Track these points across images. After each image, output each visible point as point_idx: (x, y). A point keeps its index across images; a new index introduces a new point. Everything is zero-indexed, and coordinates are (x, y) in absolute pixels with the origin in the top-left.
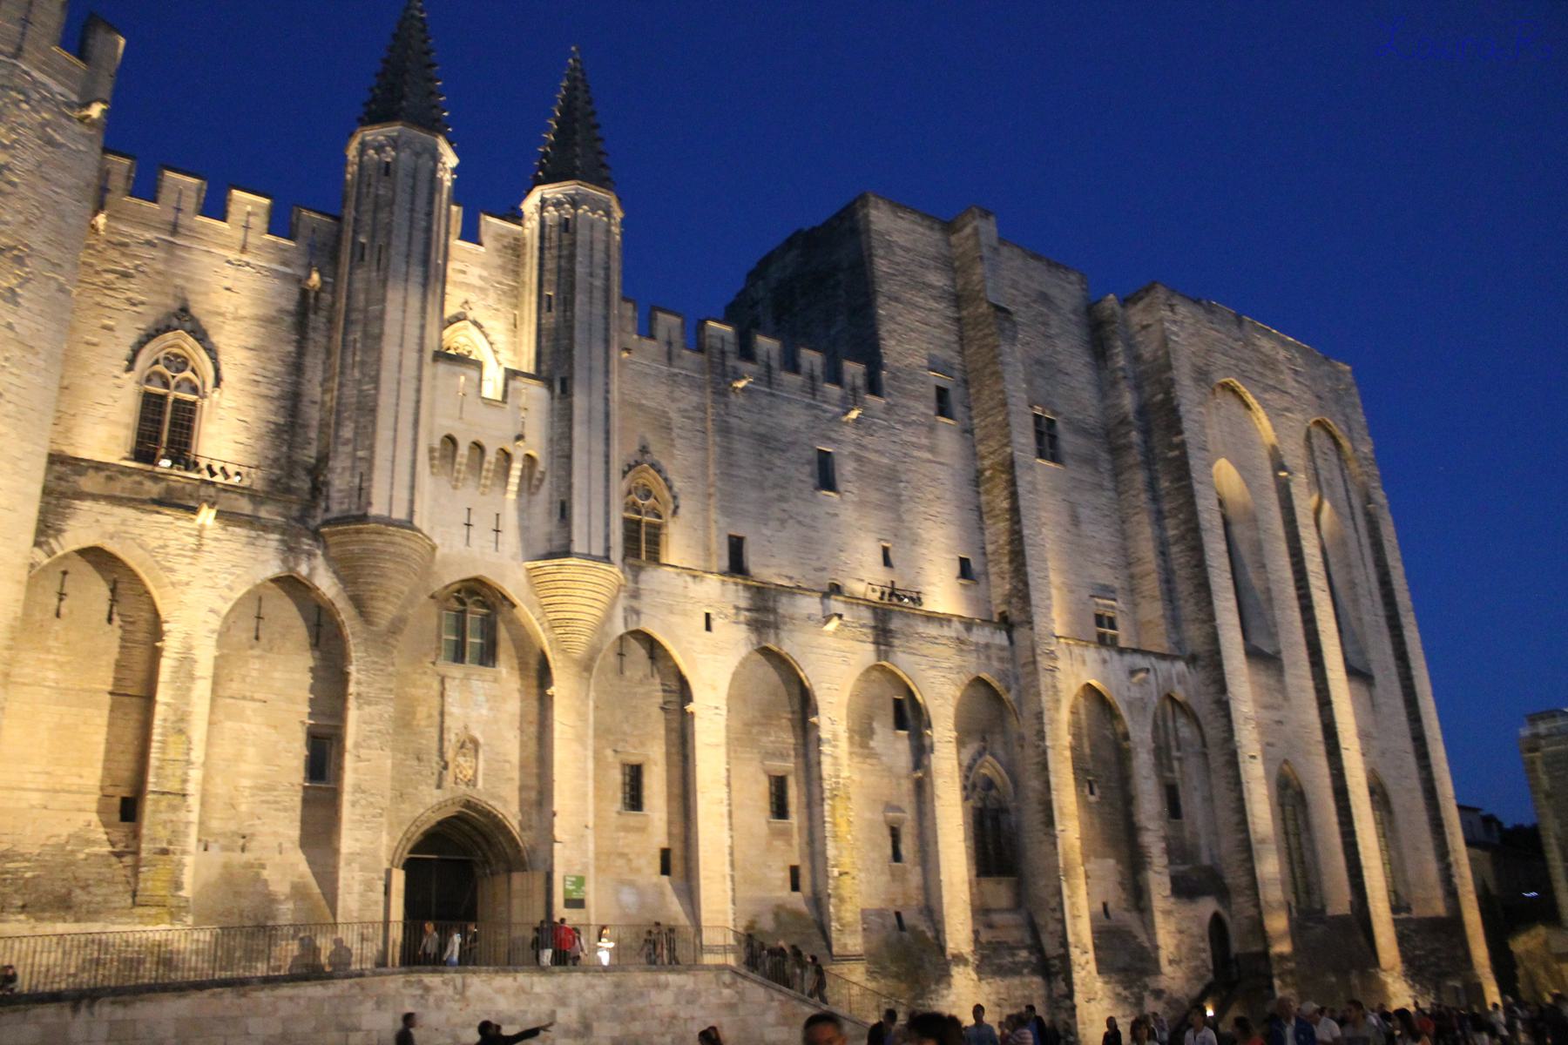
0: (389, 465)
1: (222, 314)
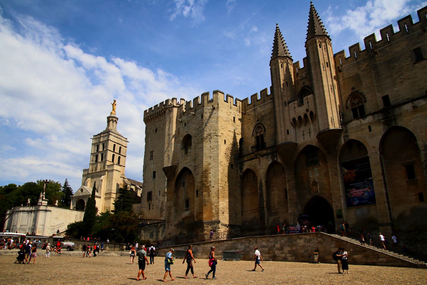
1: (263, 116)
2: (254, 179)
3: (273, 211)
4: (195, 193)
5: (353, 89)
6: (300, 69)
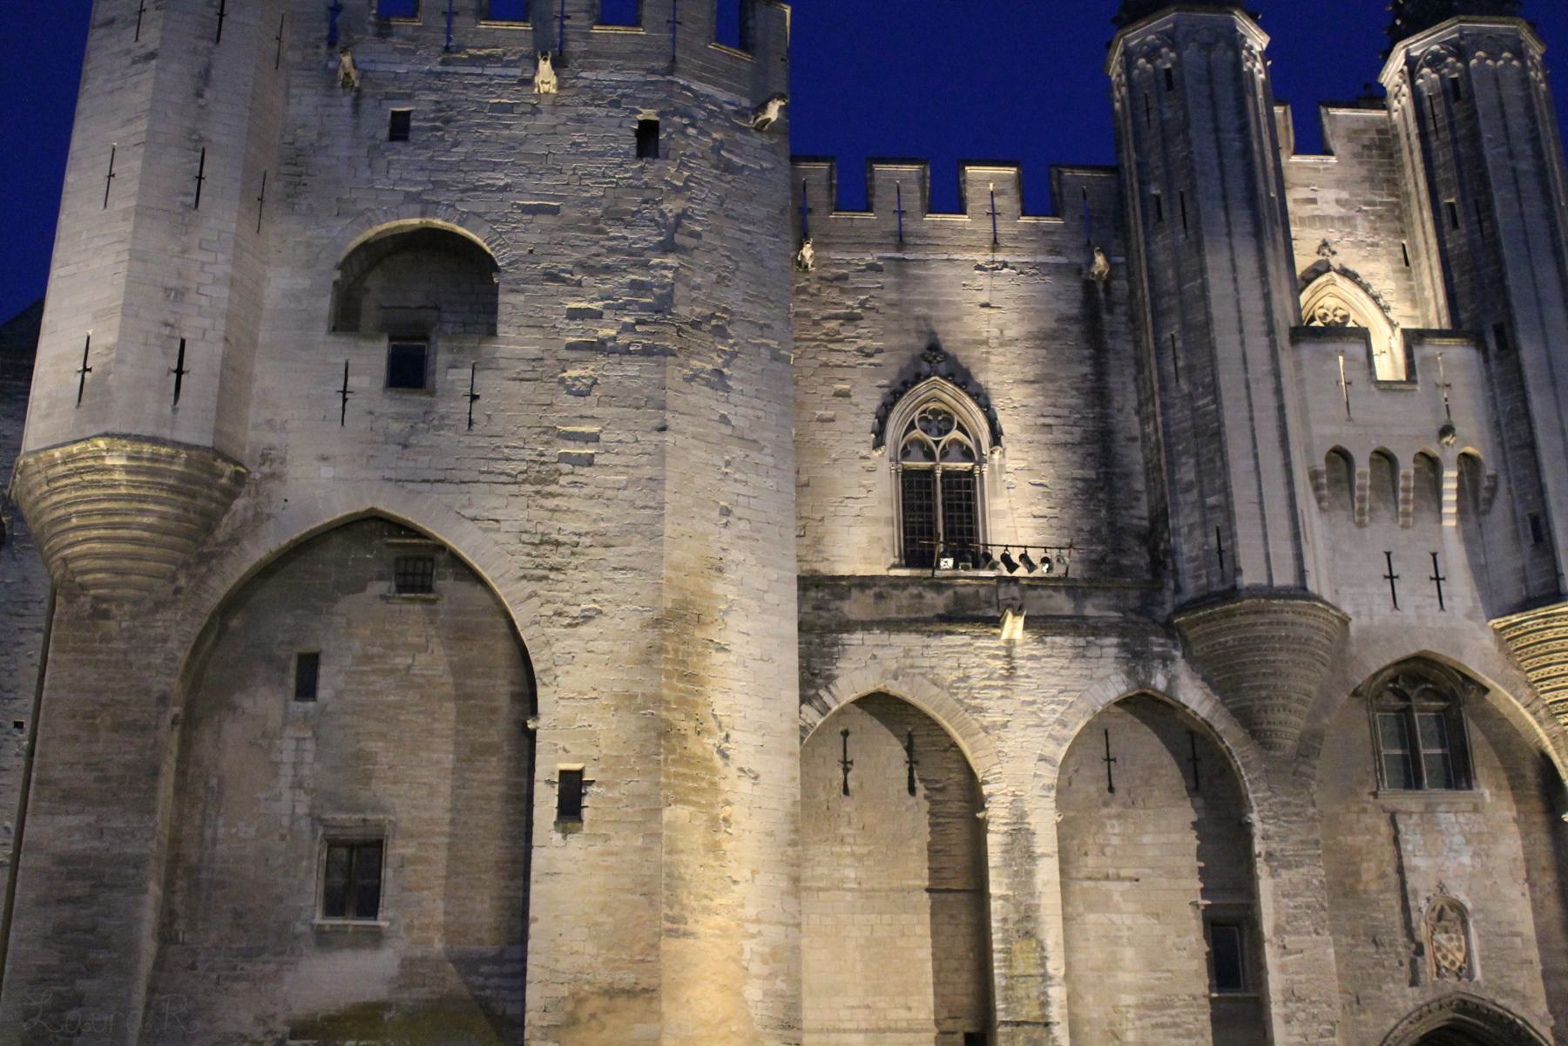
0: (1255, 509)
1: (985, 342)
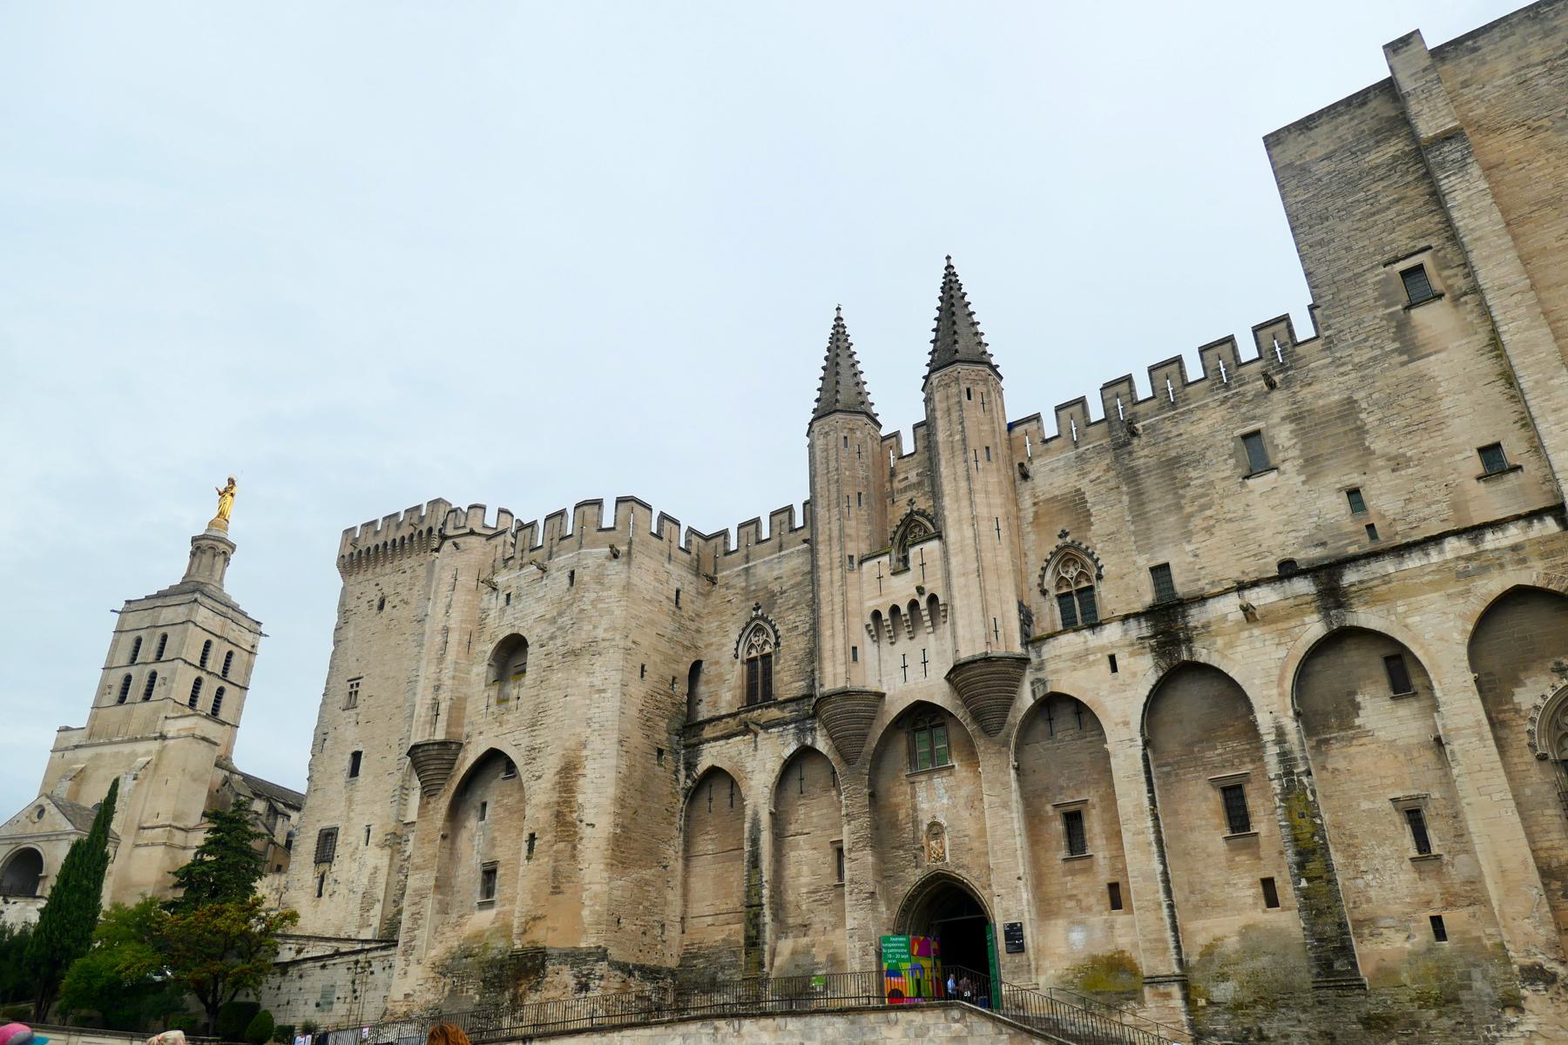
2: (732, 806)
3: (791, 921)
4: (525, 846)
5: (1064, 534)
6: (901, 457)
